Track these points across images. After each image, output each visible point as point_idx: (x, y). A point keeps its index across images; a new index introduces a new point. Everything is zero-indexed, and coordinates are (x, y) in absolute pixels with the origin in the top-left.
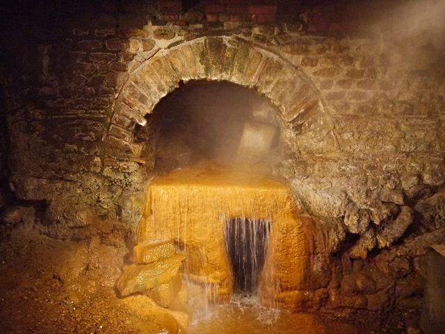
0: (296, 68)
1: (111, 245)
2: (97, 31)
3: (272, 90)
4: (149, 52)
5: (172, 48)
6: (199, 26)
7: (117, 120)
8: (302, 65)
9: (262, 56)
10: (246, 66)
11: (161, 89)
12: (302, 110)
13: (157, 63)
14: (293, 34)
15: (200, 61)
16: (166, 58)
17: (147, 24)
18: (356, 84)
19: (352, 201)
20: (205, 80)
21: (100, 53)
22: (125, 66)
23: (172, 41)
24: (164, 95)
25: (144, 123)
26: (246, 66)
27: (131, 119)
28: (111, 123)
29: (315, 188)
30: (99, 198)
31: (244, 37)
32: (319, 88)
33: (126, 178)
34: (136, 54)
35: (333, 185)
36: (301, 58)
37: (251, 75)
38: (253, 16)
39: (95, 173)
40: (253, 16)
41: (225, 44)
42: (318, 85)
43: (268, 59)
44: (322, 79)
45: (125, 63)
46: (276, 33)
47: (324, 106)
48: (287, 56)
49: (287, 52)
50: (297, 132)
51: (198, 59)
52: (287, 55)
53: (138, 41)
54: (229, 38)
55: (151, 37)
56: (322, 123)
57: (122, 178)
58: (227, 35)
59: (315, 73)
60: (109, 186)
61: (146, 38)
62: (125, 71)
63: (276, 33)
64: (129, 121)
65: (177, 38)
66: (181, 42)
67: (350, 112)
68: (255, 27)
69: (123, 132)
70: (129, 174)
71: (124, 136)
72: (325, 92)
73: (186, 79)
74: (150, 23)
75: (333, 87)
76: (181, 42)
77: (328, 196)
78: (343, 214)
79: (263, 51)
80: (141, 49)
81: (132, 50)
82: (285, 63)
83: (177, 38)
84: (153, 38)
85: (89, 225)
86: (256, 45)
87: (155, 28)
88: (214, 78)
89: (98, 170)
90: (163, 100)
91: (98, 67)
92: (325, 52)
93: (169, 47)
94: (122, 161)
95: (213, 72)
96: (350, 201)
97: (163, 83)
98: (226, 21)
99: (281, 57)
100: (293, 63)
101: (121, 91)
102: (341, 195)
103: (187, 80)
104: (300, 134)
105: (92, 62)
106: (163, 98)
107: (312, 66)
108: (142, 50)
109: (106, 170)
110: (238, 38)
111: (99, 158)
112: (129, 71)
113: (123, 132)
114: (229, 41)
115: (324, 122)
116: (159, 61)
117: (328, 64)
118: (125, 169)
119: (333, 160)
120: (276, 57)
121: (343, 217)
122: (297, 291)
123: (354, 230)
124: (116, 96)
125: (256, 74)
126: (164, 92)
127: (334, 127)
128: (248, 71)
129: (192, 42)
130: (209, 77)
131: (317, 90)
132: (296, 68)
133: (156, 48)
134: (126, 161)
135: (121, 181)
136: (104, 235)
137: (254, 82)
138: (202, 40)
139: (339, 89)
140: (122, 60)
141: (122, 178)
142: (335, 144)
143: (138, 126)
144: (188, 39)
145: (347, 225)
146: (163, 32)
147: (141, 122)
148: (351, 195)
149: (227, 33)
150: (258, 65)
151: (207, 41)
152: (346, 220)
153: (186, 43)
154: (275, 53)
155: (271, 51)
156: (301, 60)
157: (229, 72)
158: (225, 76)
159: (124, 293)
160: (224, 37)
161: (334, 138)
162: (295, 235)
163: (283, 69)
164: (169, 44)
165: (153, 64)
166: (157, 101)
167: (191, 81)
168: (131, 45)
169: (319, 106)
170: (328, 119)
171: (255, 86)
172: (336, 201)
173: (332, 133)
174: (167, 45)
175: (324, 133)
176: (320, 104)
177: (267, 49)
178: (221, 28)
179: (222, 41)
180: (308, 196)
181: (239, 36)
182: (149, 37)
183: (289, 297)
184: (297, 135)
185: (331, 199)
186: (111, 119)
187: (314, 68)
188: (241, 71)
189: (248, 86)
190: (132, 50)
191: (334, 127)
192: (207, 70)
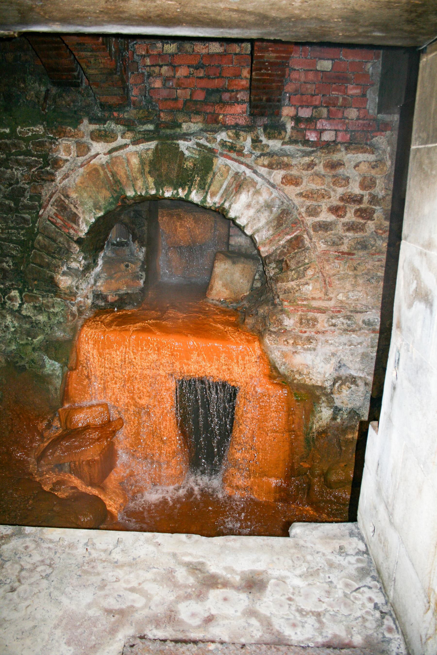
2: (19, 129)
5: (115, 154)
14: (271, 143)
18: (353, 211)
21: (22, 157)
22: (53, 175)
23: (114, 145)
24: (101, 214)
37: (213, 195)
39: (12, 312)
41: (182, 152)
45: (53, 171)
47: (311, 239)
54: (189, 144)
55: (87, 139)
58: (186, 140)
66: (126, 145)
67: (345, 248)
68: (222, 131)
76: (126, 145)
81: (63, 155)
86: (222, 155)
88: (168, 194)
90: (98, 220)
91: (19, 175)
92: (313, 168)
93: (110, 152)
97: (100, 198)
98: (184, 122)
105: (12, 168)
106: (100, 218)
108: (76, 154)
110: (198, 144)
116: (96, 170)
117: (317, 184)
118: (48, 307)
120: (248, 172)
128: (212, 188)
137: (219, 203)
139: (331, 218)
144: (135, 142)
149: (185, 136)
153: (132, 148)
155: (242, 163)
157: (187, 188)
158: (182, 193)
164: (110, 148)
166: (93, 220)
174: (106, 151)
178: (178, 130)
179: (179, 148)
192: (159, 185)
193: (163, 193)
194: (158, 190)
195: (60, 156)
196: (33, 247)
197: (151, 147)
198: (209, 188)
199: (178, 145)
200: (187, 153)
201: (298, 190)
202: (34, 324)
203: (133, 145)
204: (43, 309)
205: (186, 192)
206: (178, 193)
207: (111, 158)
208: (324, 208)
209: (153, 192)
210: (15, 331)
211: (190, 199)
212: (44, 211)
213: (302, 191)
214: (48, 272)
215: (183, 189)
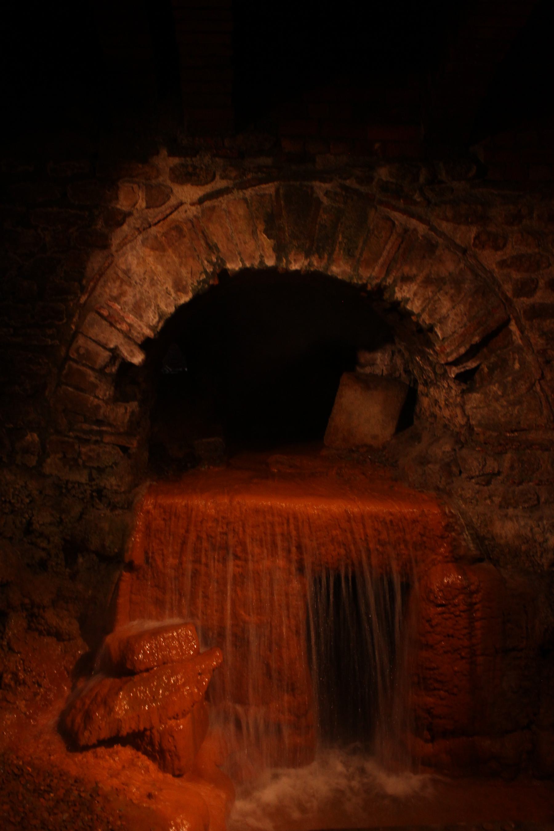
0: (464, 251)
1: (49, 634)
3: (415, 294)
4: (157, 210)
5: (207, 204)
6: (268, 161)
7: (82, 351)
8: (475, 245)
9: (394, 224)
10: (361, 245)
11: (179, 287)
12: (477, 339)
13: (174, 233)
15: (266, 232)
16: (193, 223)
17: (157, 153)
20: (273, 270)
23: (208, 188)
24: (185, 299)
25: (138, 359)
26: (361, 245)
27: (111, 350)
28: (67, 358)
30: (30, 523)
31: (357, 186)
32: (509, 294)
33: (91, 479)
34: (130, 214)
36: (474, 231)
38: (377, 145)
40: (377, 145)
42: (508, 289)
43: (406, 231)
44: (516, 275)
46: (422, 179)
47: (522, 332)
48: (445, 226)
49: (447, 220)
50: (464, 387)
51: (261, 227)
52: (444, 224)
53: (135, 186)
54: (327, 186)
55: (165, 179)
56: (517, 366)
57: (84, 479)
59: (502, 264)
61: (154, 182)
62: (106, 246)
63: (422, 179)
64: (107, 354)
65: (220, 184)
66: (226, 191)
69: (92, 377)
70: (101, 470)
71: (95, 386)
72: (524, 301)
73: (234, 266)
74: (164, 152)
75: (539, 294)
79: (397, 216)
80: (142, 204)
81: (123, 205)
82: (441, 241)
83: (220, 184)
84: (169, 183)
87: (175, 161)
88: (295, 267)
89: (33, 461)
90: (181, 309)
93: (201, 201)
94: (87, 441)
95: (291, 257)
99: (432, 228)
100: (458, 241)
101: (94, 289)
103: (237, 269)
104: (471, 390)
107: (497, 248)
108: (144, 205)
109: (49, 461)
111: (35, 436)
112: (113, 249)
113: (92, 377)
114: (327, 194)
115: (522, 363)
116: (178, 228)
120: (422, 228)
124: (83, 299)
125: (381, 260)
126: (186, 293)
127: (543, 377)
129: (249, 193)
130: (284, 264)
131: (507, 298)
132: (464, 251)
133: (173, 201)
134: (96, 442)
138: (270, 188)
140: (99, 225)
141: (84, 479)
142: (545, 412)
143: (126, 366)
144: (242, 186)
146: (190, 169)
147: (133, 356)
150: (386, 243)
151: (281, 191)
153: (238, 194)
154: (420, 219)
155: (412, 215)
156: (473, 235)
157: (326, 256)
158: (317, 264)
159: (87, 737)
160: (316, 184)
163: (438, 253)
165: (165, 234)
166: (172, 310)
167: (244, 271)
168: (121, 196)
169: (510, 332)
170: (530, 358)
171: (379, 286)
173: (538, 388)
175: (523, 387)
176: (513, 327)
177: (404, 212)
181: (348, 183)
182: (161, 179)
184: (463, 392)
187: (499, 253)
188: (349, 253)
189: (365, 286)
190: (123, 205)
191: (543, 377)
193: (289, 262)
194: (279, 259)
195: (119, 207)
196: (67, 358)
197: (267, 192)
198: (361, 254)
199: (312, 188)
200: (325, 201)
201: (499, 256)
202: (64, 491)
203: (238, 189)
204: (80, 462)
205: (325, 261)
206: (310, 264)
207: (203, 211)
208: (541, 283)
209: (270, 262)
210: (31, 501)
211: (329, 274)
212: (89, 296)
213: (505, 258)
214: (92, 398)
215: (321, 258)
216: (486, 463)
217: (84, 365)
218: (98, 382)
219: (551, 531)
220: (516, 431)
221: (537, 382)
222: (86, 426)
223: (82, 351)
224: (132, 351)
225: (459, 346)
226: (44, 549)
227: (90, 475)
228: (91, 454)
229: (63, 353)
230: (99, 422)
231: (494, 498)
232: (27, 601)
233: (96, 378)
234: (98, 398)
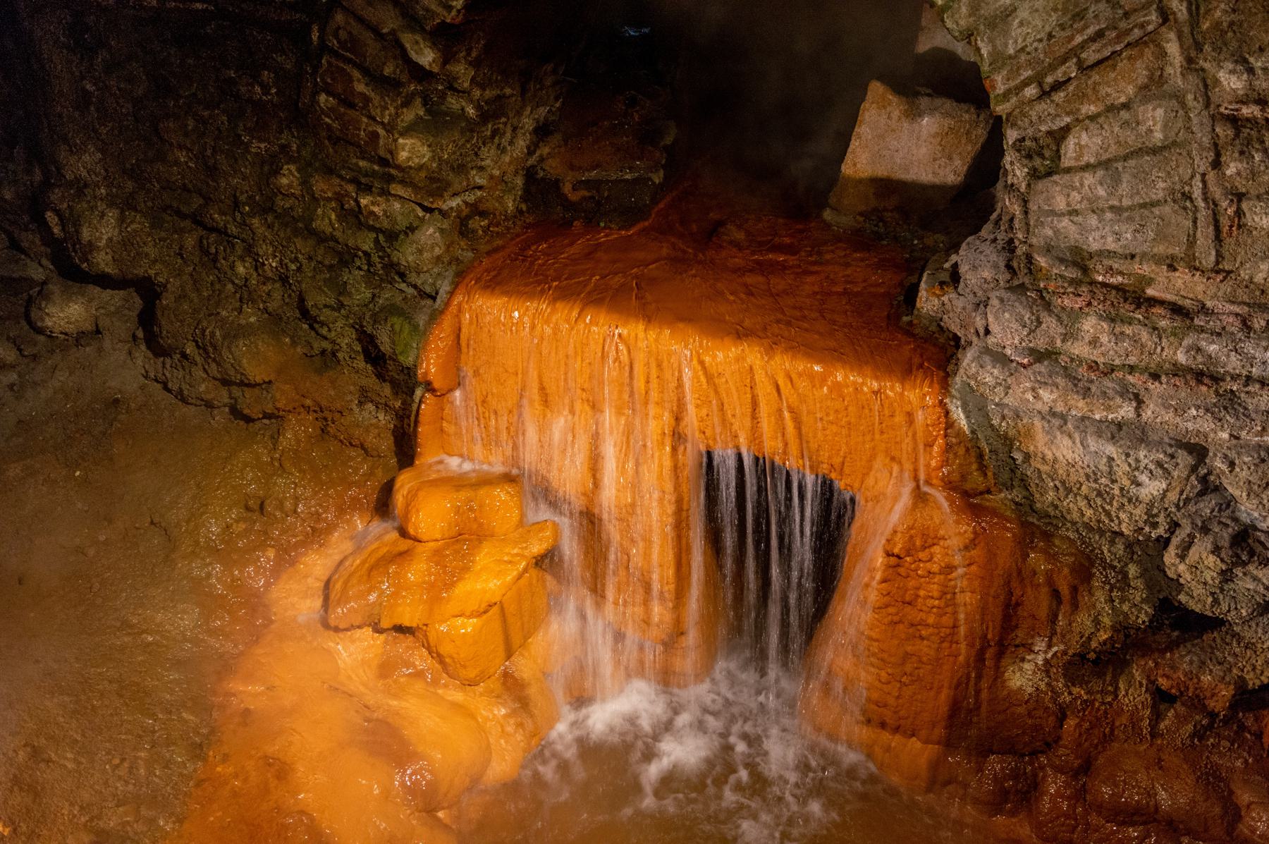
19: (1218, 489)
29: (1060, 408)
35: (1147, 414)
57: (368, 245)
60: (331, 267)
77: (1111, 450)
78: (1161, 531)
85: (270, 382)
94: (368, 189)
96: (1208, 487)
102: (1172, 456)
119: (1177, 310)
121: (1164, 543)
122: (915, 744)
123: (1196, 598)
135: (365, 253)
136: (327, 414)
145: (1171, 574)
148: (1219, 464)
152: (1170, 557)
161: (1203, 214)
162: (935, 568)
172: (1143, 478)
180: (1029, 434)
183: (888, 749)
185: (1122, 468)
186: (322, 30)
196: (323, 47)
216: (1040, 323)
217: (349, 61)
218: (373, 95)
219: (1151, 472)
220: (1121, 273)
221: (1198, 177)
222: (362, 163)
223: (343, 35)
224: (417, 43)
225: (1026, 83)
226: (325, 338)
227: (377, 241)
228: (376, 209)
229: (315, 36)
230: (384, 162)
231: (1041, 392)
232: (308, 402)
233: (367, 85)
234: (374, 119)
